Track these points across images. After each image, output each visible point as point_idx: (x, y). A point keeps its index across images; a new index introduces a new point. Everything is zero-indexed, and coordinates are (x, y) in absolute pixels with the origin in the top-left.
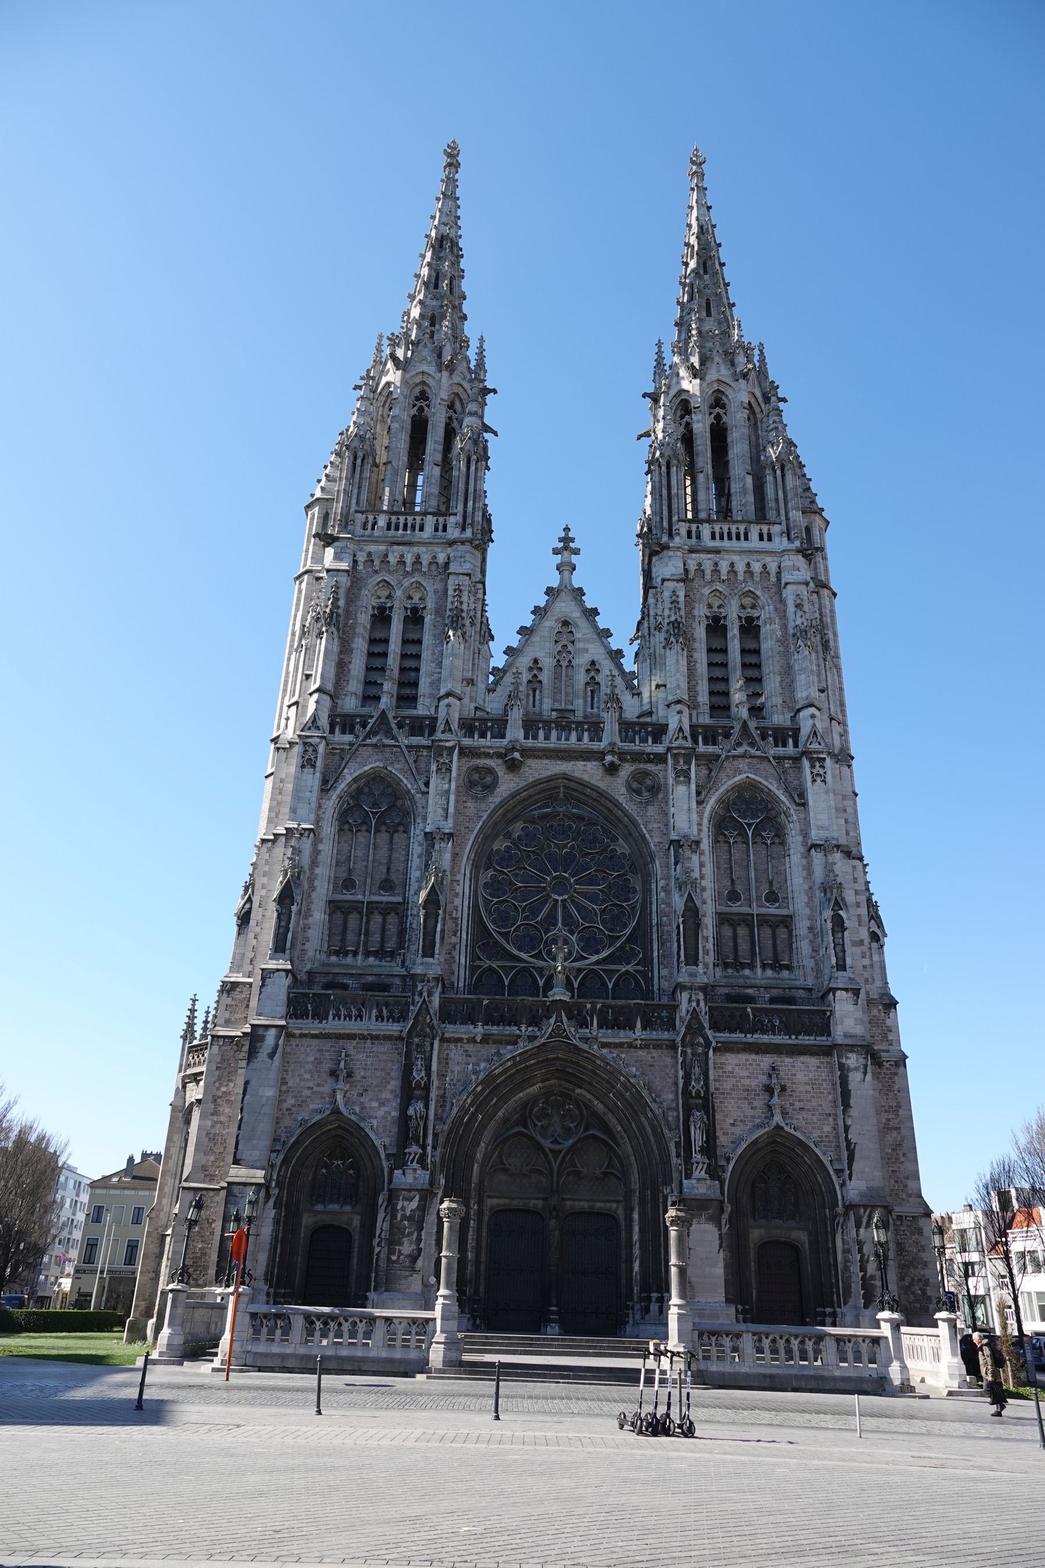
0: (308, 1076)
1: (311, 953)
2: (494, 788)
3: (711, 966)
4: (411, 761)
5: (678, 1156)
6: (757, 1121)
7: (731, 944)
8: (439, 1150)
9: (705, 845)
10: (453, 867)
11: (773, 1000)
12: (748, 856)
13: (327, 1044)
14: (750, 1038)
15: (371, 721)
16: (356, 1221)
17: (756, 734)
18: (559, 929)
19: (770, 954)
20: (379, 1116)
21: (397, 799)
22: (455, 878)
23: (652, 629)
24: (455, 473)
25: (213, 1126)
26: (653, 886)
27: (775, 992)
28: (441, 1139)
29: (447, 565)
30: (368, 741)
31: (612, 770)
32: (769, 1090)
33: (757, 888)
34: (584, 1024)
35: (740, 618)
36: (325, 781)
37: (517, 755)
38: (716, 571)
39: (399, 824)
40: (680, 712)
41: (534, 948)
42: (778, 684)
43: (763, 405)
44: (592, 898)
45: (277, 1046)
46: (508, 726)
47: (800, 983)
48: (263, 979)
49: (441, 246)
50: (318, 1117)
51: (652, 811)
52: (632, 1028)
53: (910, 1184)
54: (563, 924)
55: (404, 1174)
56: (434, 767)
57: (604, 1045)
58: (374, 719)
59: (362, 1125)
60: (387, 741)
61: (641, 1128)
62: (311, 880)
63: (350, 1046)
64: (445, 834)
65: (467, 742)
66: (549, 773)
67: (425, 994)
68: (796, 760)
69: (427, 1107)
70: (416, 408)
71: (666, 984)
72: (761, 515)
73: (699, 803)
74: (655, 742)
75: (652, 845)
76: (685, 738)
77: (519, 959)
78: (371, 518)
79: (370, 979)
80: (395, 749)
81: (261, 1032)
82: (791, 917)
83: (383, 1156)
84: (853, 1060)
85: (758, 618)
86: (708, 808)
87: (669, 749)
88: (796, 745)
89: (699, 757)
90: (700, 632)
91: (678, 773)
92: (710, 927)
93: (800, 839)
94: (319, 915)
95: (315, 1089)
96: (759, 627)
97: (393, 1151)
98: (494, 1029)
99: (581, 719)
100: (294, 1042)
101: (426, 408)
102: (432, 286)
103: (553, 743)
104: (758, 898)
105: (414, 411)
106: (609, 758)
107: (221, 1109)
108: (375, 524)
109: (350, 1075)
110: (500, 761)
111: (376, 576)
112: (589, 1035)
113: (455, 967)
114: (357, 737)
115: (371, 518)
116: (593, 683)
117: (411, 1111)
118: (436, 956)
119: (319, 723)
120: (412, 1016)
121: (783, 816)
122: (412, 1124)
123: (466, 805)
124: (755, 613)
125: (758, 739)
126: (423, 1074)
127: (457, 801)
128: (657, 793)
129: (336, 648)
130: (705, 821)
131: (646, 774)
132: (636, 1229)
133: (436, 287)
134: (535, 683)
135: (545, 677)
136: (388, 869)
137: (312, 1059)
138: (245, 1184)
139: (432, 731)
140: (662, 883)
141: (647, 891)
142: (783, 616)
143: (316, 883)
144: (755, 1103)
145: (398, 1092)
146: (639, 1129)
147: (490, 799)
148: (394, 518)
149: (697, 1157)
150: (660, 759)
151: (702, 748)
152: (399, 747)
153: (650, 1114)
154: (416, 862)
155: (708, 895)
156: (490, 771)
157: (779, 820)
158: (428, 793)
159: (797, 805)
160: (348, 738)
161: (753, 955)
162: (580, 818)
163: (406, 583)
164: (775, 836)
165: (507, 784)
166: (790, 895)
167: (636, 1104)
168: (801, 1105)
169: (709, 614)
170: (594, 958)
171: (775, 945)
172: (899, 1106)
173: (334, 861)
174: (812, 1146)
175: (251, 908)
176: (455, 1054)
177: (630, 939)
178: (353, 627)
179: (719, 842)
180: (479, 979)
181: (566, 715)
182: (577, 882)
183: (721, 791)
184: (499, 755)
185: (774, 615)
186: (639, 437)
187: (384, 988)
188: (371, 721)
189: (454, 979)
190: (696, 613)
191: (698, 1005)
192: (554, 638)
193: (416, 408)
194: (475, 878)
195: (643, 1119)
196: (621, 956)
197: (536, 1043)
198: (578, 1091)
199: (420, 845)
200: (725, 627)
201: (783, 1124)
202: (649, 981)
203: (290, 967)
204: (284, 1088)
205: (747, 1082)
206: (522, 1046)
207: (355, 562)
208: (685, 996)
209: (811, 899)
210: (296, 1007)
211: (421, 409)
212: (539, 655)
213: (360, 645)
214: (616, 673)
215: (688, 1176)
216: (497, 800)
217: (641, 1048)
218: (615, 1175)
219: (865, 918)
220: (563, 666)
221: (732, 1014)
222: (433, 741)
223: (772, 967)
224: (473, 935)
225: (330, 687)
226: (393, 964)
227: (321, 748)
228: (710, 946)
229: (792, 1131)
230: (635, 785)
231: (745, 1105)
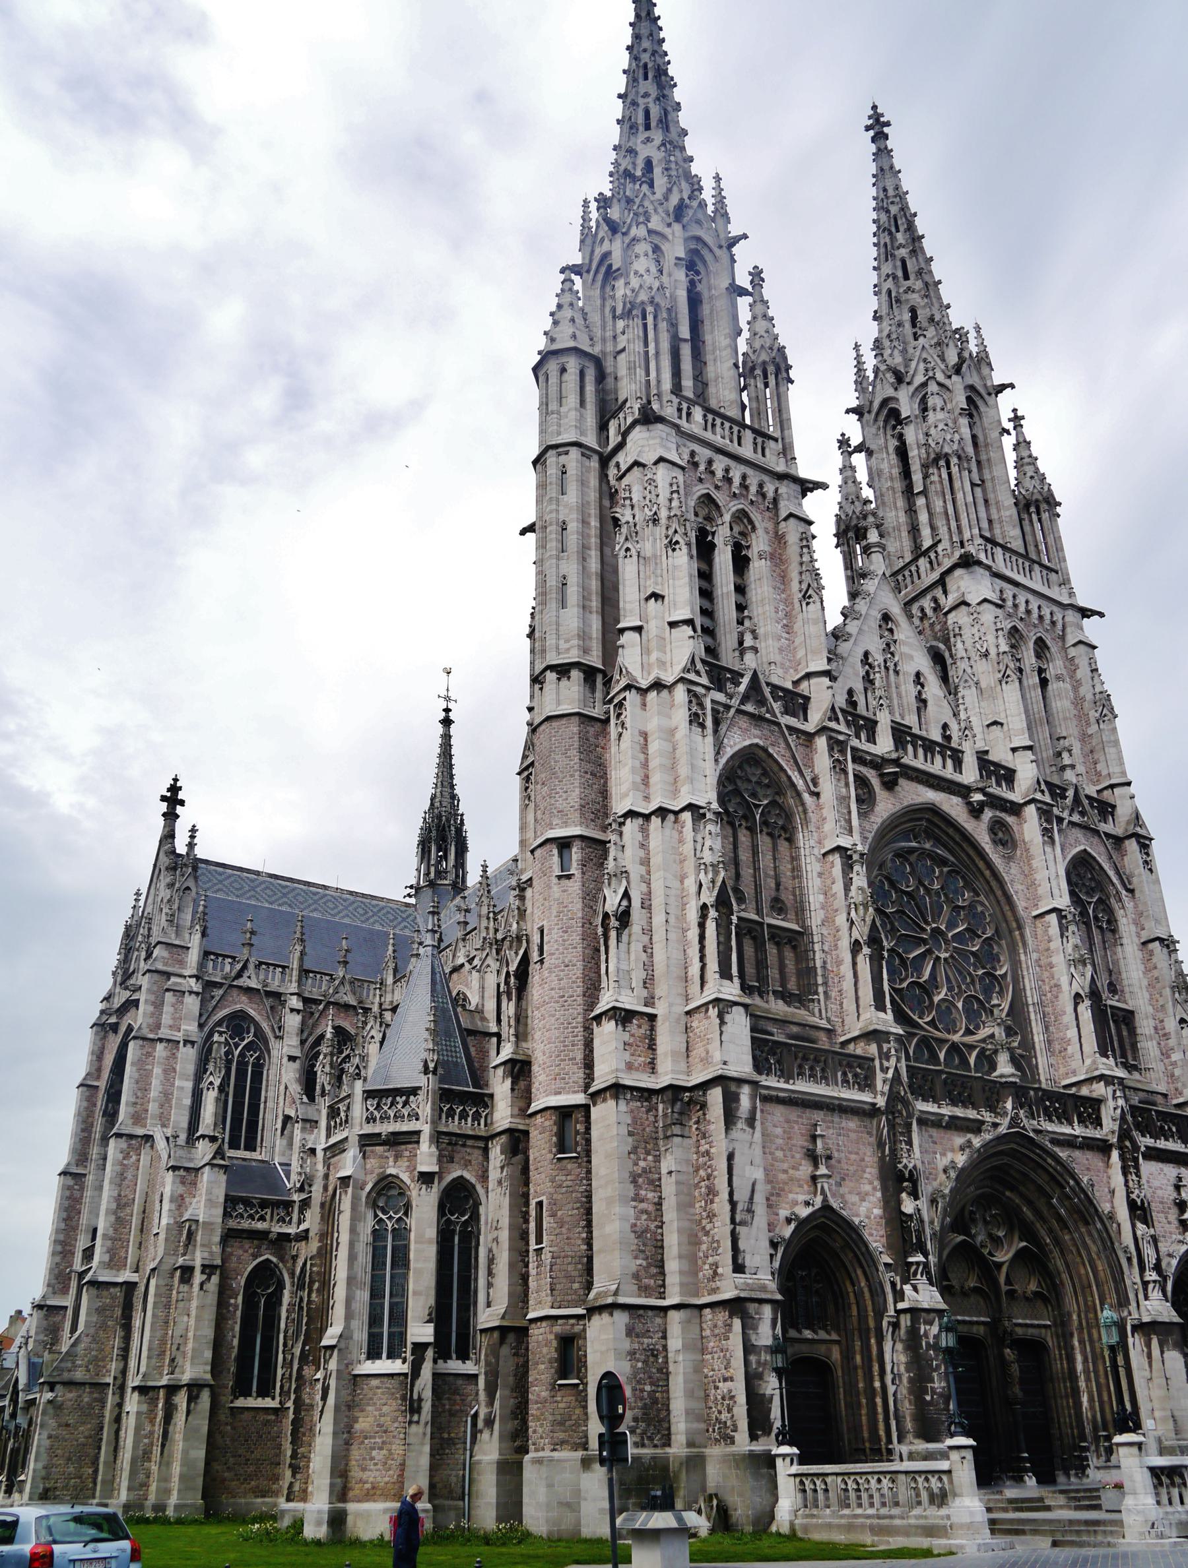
0: (779, 1154)
13: (793, 1113)
15: (745, 681)
16: (836, 1354)
25: (638, 1218)
31: (976, 811)
39: (783, 828)
51: (1014, 869)
55: (915, 1289)
63: (818, 1116)
66: (920, 800)
76: (1042, 792)
79: (795, 1029)
81: (733, 1088)
98: (959, 1112)
107: (643, 1192)
109: (829, 1158)
110: (873, 772)
111: (700, 486)
132: (1079, 1358)
134: (868, 680)
136: (778, 885)
137: (779, 1131)
138: (761, 1301)
141: (1016, 964)
145: (877, 1183)
153: (1099, 1226)
162: (943, 862)
163: (735, 506)
167: (1086, 1210)
175: (629, 907)
186: (848, 411)
188: (745, 681)
192: (877, 631)
198: (1008, 1193)
206: (988, 1137)
212: (872, 649)
216: (879, 821)
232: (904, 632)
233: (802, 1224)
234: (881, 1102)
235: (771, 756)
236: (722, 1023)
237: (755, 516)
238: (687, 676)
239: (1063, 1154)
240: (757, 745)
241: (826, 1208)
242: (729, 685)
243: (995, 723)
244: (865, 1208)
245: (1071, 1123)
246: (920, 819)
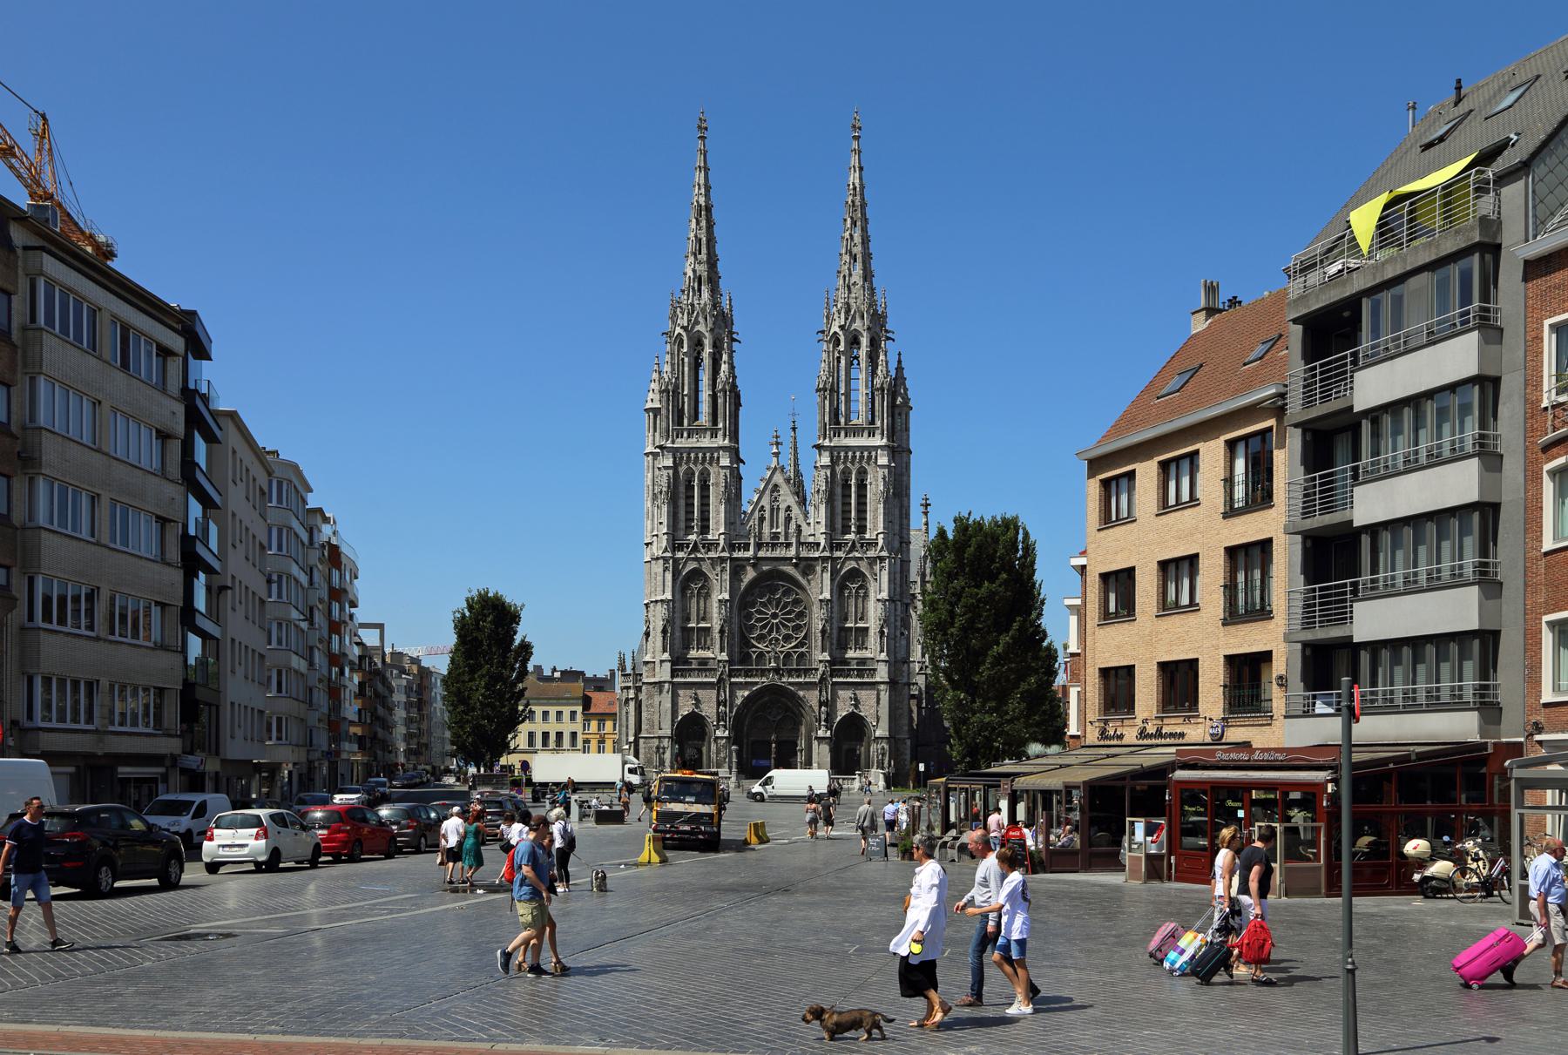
18: (774, 634)
20: (709, 710)
31: (796, 565)
38: (846, 457)
44: (789, 620)
84: (882, 687)
89: (834, 560)
94: (678, 634)
103: (769, 554)
116: (788, 519)
134: (762, 519)
135: (767, 515)
150: (816, 559)
151: (838, 554)
154: (715, 610)
165: (750, 574)
177: (805, 637)
184: (748, 559)
196: (801, 644)
210: (674, 673)
213: (682, 503)
220: (774, 510)
233: (684, 717)
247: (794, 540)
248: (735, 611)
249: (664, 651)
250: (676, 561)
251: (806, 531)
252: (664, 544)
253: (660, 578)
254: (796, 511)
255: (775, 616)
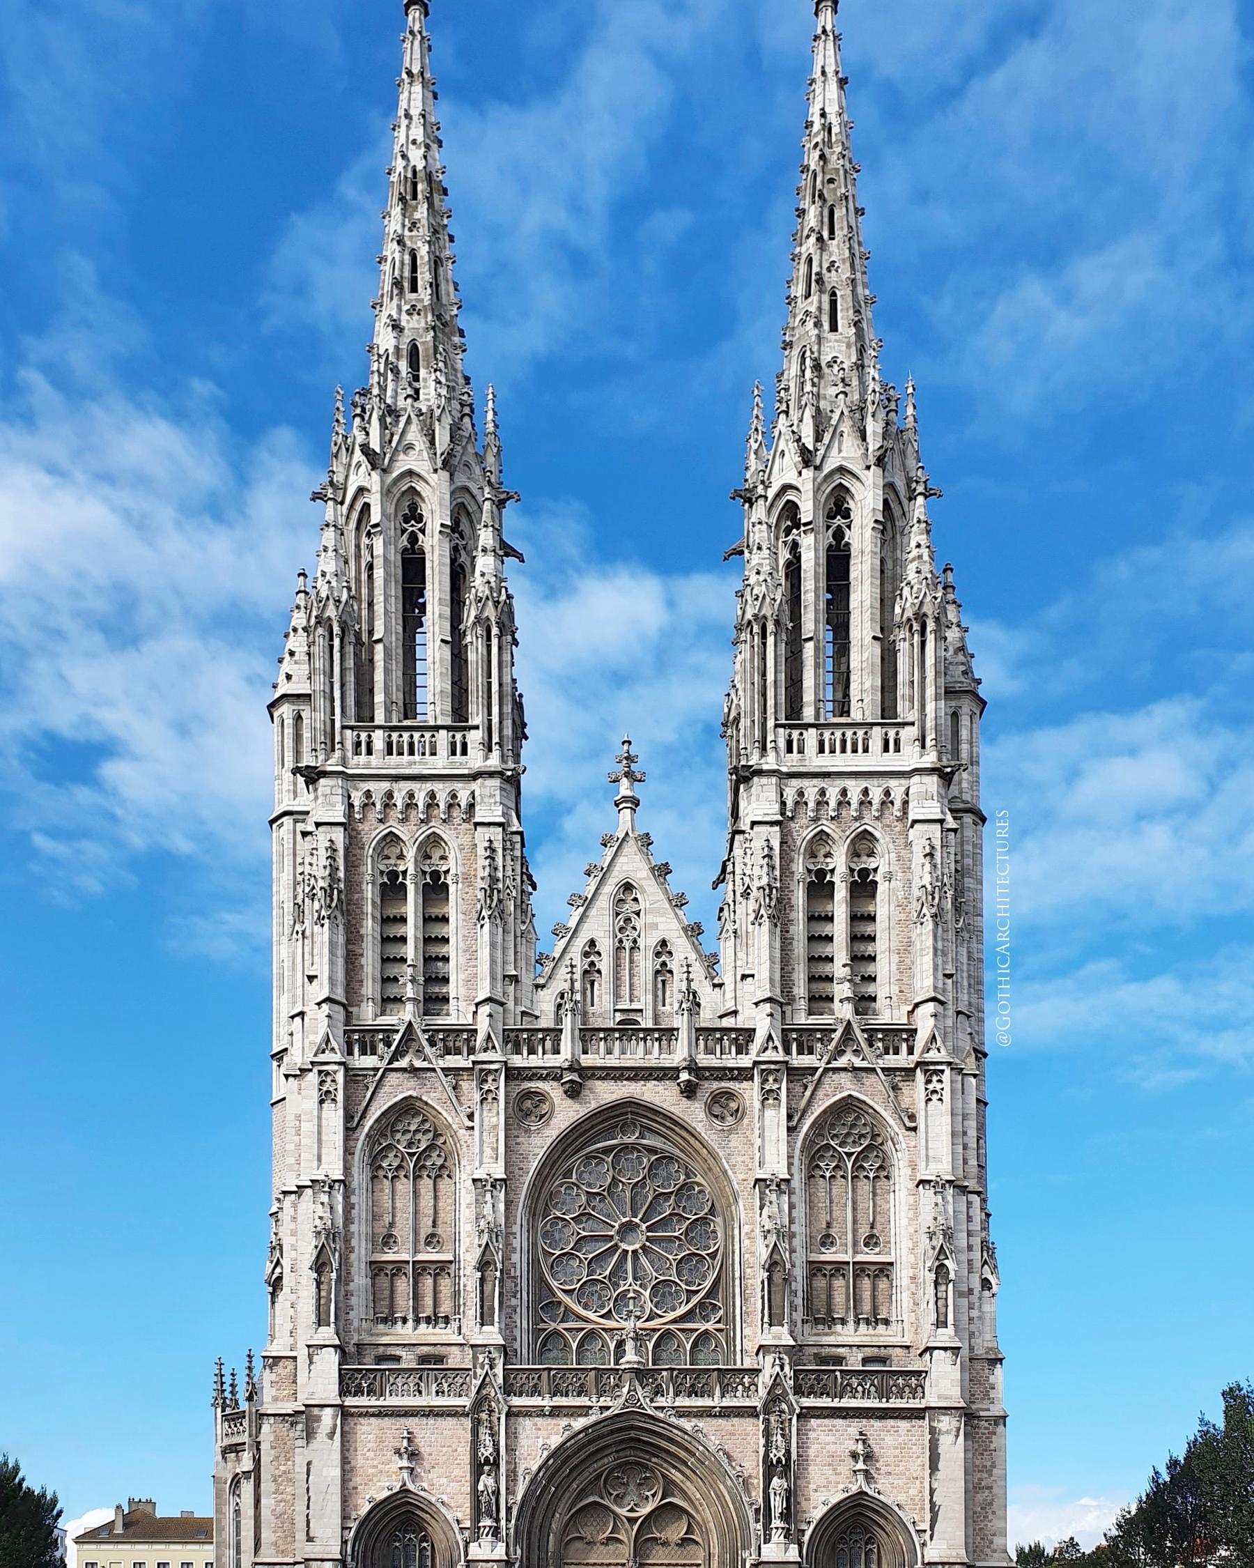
1: (356, 1324)
2: (550, 1118)
3: (799, 1323)
4: (449, 1089)
5: (757, 1521)
6: (841, 1486)
7: (824, 1296)
8: (513, 1522)
9: (796, 1183)
10: (507, 1218)
11: (865, 1361)
12: (847, 1192)
14: (836, 1403)
15: (397, 1037)
17: (861, 1037)
19: (867, 1306)
21: (437, 1135)
22: (509, 1230)
23: (738, 894)
24: (472, 657)
26: (736, 1232)
27: (869, 1352)
28: (515, 1512)
29: (472, 806)
30: (396, 1065)
31: (689, 1091)
32: (854, 1456)
33: (855, 1231)
34: (658, 1392)
35: (852, 870)
36: (348, 1117)
37: (574, 1076)
38: (821, 803)
39: (442, 1166)
40: (771, 1015)
41: (603, 1307)
42: (894, 967)
43: (905, 502)
45: (335, 1426)
46: (563, 1037)
47: (897, 1340)
48: (310, 1357)
49: (415, 197)
50: (386, 1494)
51: (735, 1141)
52: (711, 1395)
53: (997, 1541)
54: (635, 1279)
56: (477, 1097)
57: (683, 1413)
58: (400, 1034)
59: (433, 1500)
60: (418, 1064)
61: (720, 1497)
62: (347, 1240)
63: (411, 1422)
64: (496, 1180)
65: (518, 1061)
66: (614, 1097)
67: (487, 1367)
68: (909, 1073)
69: (497, 1481)
70: (406, 536)
71: (750, 1344)
72: (888, 709)
73: (791, 1130)
74: (739, 1052)
75: (735, 1183)
77: (586, 1320)
78: (364, 736)
80: (429, 1074)
82: (891, 1264)
83: (457, 1531)
85: (875, 870)
86: (802, 1135)
87: (756, 1063)
88: (911, 1051)
90: (799, 896)
91: (767, 1095)
92: (799, 1279)
93: (909, 1171)
94: (360, 1280)
95: (380, 1466)
96: (876, 883)
97: (467, 1524)
99: (650, 1025)
100: (351, 1421)
101: (420, 536)
102: (406, 285)
104: (855, 1243)
105: (404, 541)
106: (684, 1076)
108: (369, 744)
110: (555, 1084)
112: (665, 1404)
113: (517, 1333)
114: (382, 1058)
115: (364, 736)
116: (663, 971)
117: (481, 1487)
118: (496, 1324)
119: (334, 1044)
120: (474, 1390)
121: (890, 1142)
122: (483, 1499)
123: (519, 1140)
124: (871, 863)
125: (864, 1045)
126: (491, 1450)
127: (506, 1137)
128: (742, 1118)
129: (341, 940)
130: (797, 1153)
131: (730, 1095)
133: (414, 289)
139: (471, 1051)
140: (745, 1229)
141: (728, 1238)
142: (907, 869)
143: (354, 1242)
144: (840, 1469)
146: (718, 1497)
147: (547, 1132)
148: (395, 735)
149: (776, 1523)
150: (743, 1074)
152: (434, 1070)
153: (729, 1482)
155: (796, 1242)
156: (542, 1097)
157: (884, 1148)
158: (472, 1128)
159: (909, 1129)
160: (369, 1061)
161: (848, 1309)
162: (651, 1150)
163: (423, 833)
164: (881, 1167)
165: (566, 1113)
166: (893, 1240)
168: (889, 1469)
169: (811, 867)
170: (672, 1315)
171: (874, 1297)
172: (994, 1466)
173: (370, 1214)
174: (896, 1509)
176: (526, 1426)
178: (359, 905)
179: (813, 1176)
180: (544, 1344)
181: (632, 1016)
182: (649, 1229)
183: (816, 1114)
184: (553, 1075)
185: (895, 868)
187: (440, 1359)
189: (517, 1345)
190: (794, 867)
191: (782, 1369)
193: (406, 536)
194: (532, 1228)
195: (721, 1487)
197: (607, 1413)
198: (654, 1460)
199: (468, 1192)
200: (832, 884)
201: (866, 1489)
202: (731, 1341)
203: (337, 1342)
204: (347, 1467)
205: (832, 1448)
206: (592, 1419)
207: (351, 806)
208: (769, 1358)
209: (916, 1244)
211: (413, 539)
214: (693, 956)
215: (767, 1541)
216: (557, 1132)
217: (720, 1416)
218: (694, 1541)
219: (978, 1264)
221: (815, 1374)
222: (474, 1062)
223: (868, 1322)
224: (534, 1294)
225: (340, 995)
226: (448, 1330)
227: (340, 1077)
228: (799, 1301)
229: (876, 1495)
230: (717, 1110)
231: (828, 1471)
232: (651, 895)
233: (377, 1506)
234: (468, 1404)
235: (426, 1103)
236: (311, 1363)
237: (445, 832)
238: (316, 1059)
239: (687, 1424)
240: (411, 1096)
241: (404, 1491)
242: (381, 1045)
243: (744, 977)
244: (447, 1488)
245: (711, 1395)
246: (627, 1113)
247: (681, 1022)
248: (520, 1211)
249: (321, 1321)
250: (353, 1076)
251: (712, 1005)
252: (322, 1028)
253: (309, 1127)
254: (682, 949)
255: (628, 1228)
